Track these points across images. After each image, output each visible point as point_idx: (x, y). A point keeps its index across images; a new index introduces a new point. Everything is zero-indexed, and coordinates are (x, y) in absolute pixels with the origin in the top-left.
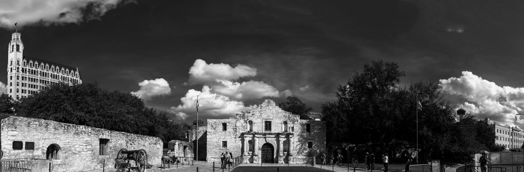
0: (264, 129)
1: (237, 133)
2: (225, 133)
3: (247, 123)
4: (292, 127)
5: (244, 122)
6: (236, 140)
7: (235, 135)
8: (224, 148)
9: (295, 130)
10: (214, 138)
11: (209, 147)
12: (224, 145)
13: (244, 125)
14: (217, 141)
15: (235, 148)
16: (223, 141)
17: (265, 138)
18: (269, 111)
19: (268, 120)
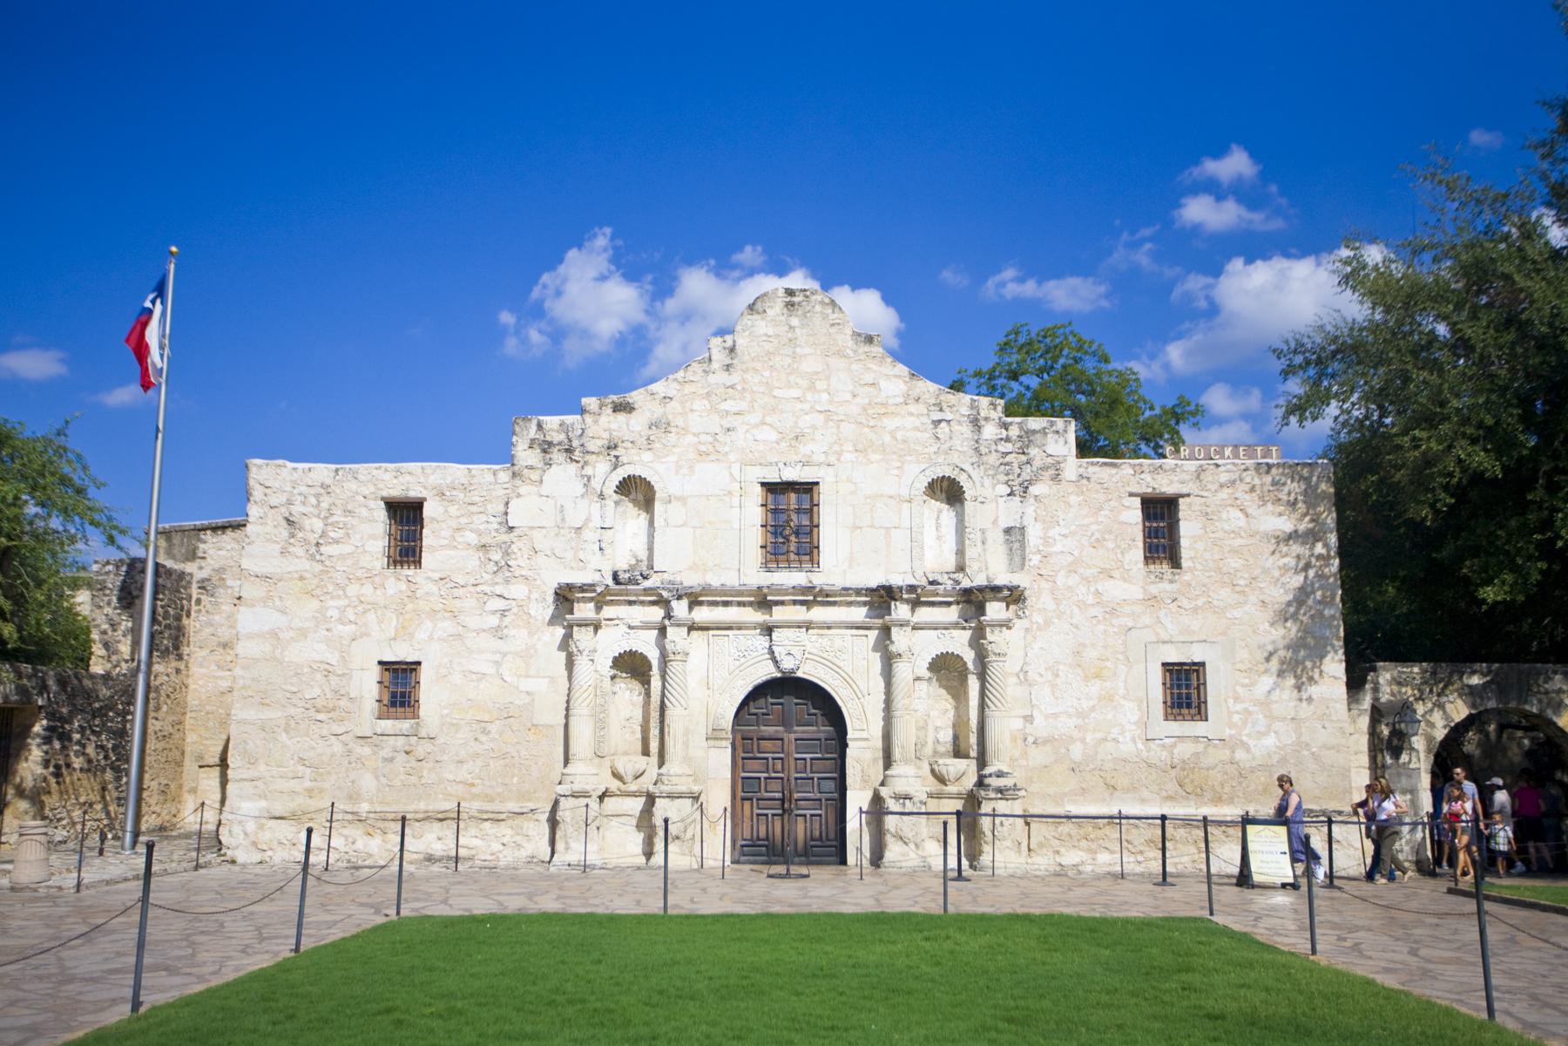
0: (755, 555)
1: (518, 590)
2: (403, 586)
3: (602, 496)
4: (1008, 531)
5: (580, 489)
6: (505, 655)
7: (499, 604)
8: (387, 725)
9: (1035, 560)
10: (303, 633)
11: (251, 714)
12: (394, 695)
13: (575, 519)
14: (333, 658)
15: (493, 728)
16: (380, 663)
17: (768, 630)
18: (795, 393)
19: (790, 475)
